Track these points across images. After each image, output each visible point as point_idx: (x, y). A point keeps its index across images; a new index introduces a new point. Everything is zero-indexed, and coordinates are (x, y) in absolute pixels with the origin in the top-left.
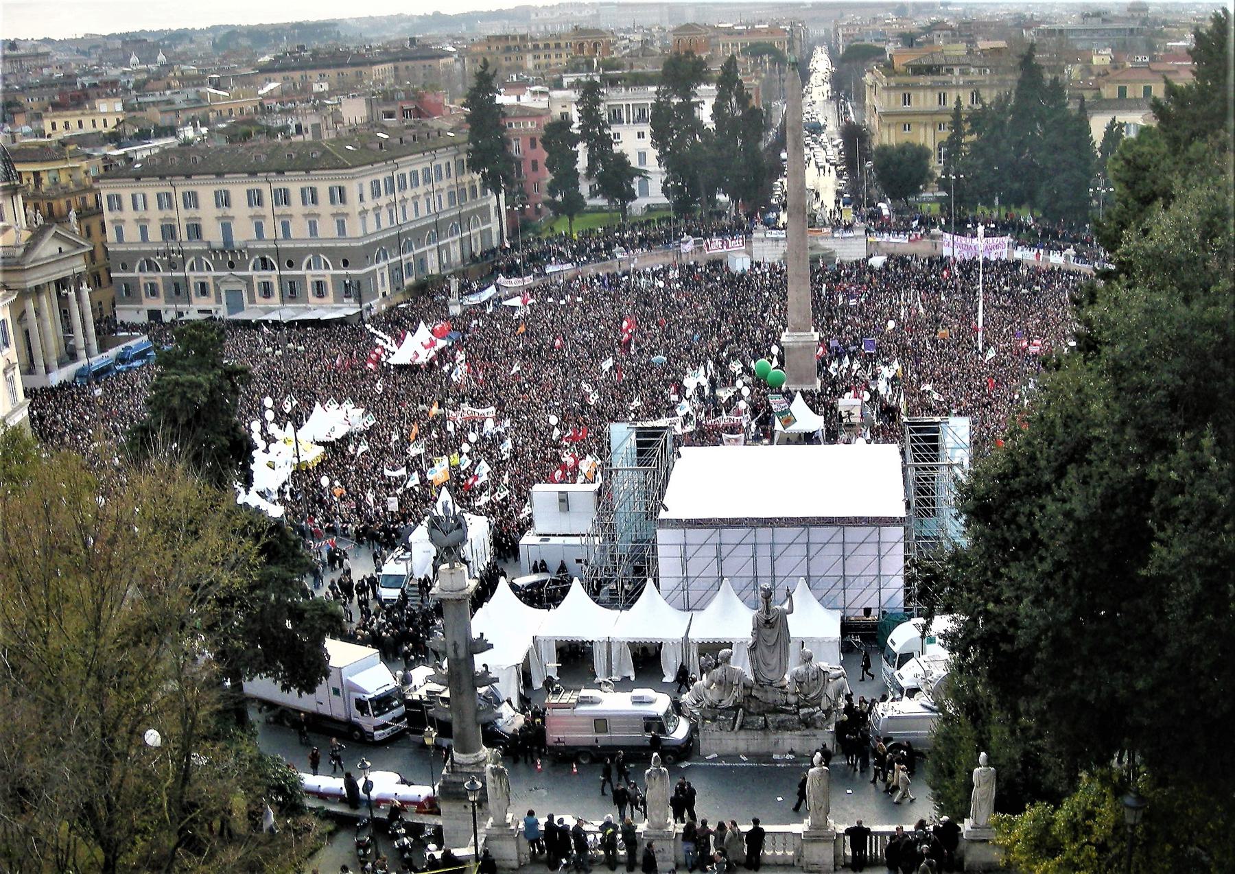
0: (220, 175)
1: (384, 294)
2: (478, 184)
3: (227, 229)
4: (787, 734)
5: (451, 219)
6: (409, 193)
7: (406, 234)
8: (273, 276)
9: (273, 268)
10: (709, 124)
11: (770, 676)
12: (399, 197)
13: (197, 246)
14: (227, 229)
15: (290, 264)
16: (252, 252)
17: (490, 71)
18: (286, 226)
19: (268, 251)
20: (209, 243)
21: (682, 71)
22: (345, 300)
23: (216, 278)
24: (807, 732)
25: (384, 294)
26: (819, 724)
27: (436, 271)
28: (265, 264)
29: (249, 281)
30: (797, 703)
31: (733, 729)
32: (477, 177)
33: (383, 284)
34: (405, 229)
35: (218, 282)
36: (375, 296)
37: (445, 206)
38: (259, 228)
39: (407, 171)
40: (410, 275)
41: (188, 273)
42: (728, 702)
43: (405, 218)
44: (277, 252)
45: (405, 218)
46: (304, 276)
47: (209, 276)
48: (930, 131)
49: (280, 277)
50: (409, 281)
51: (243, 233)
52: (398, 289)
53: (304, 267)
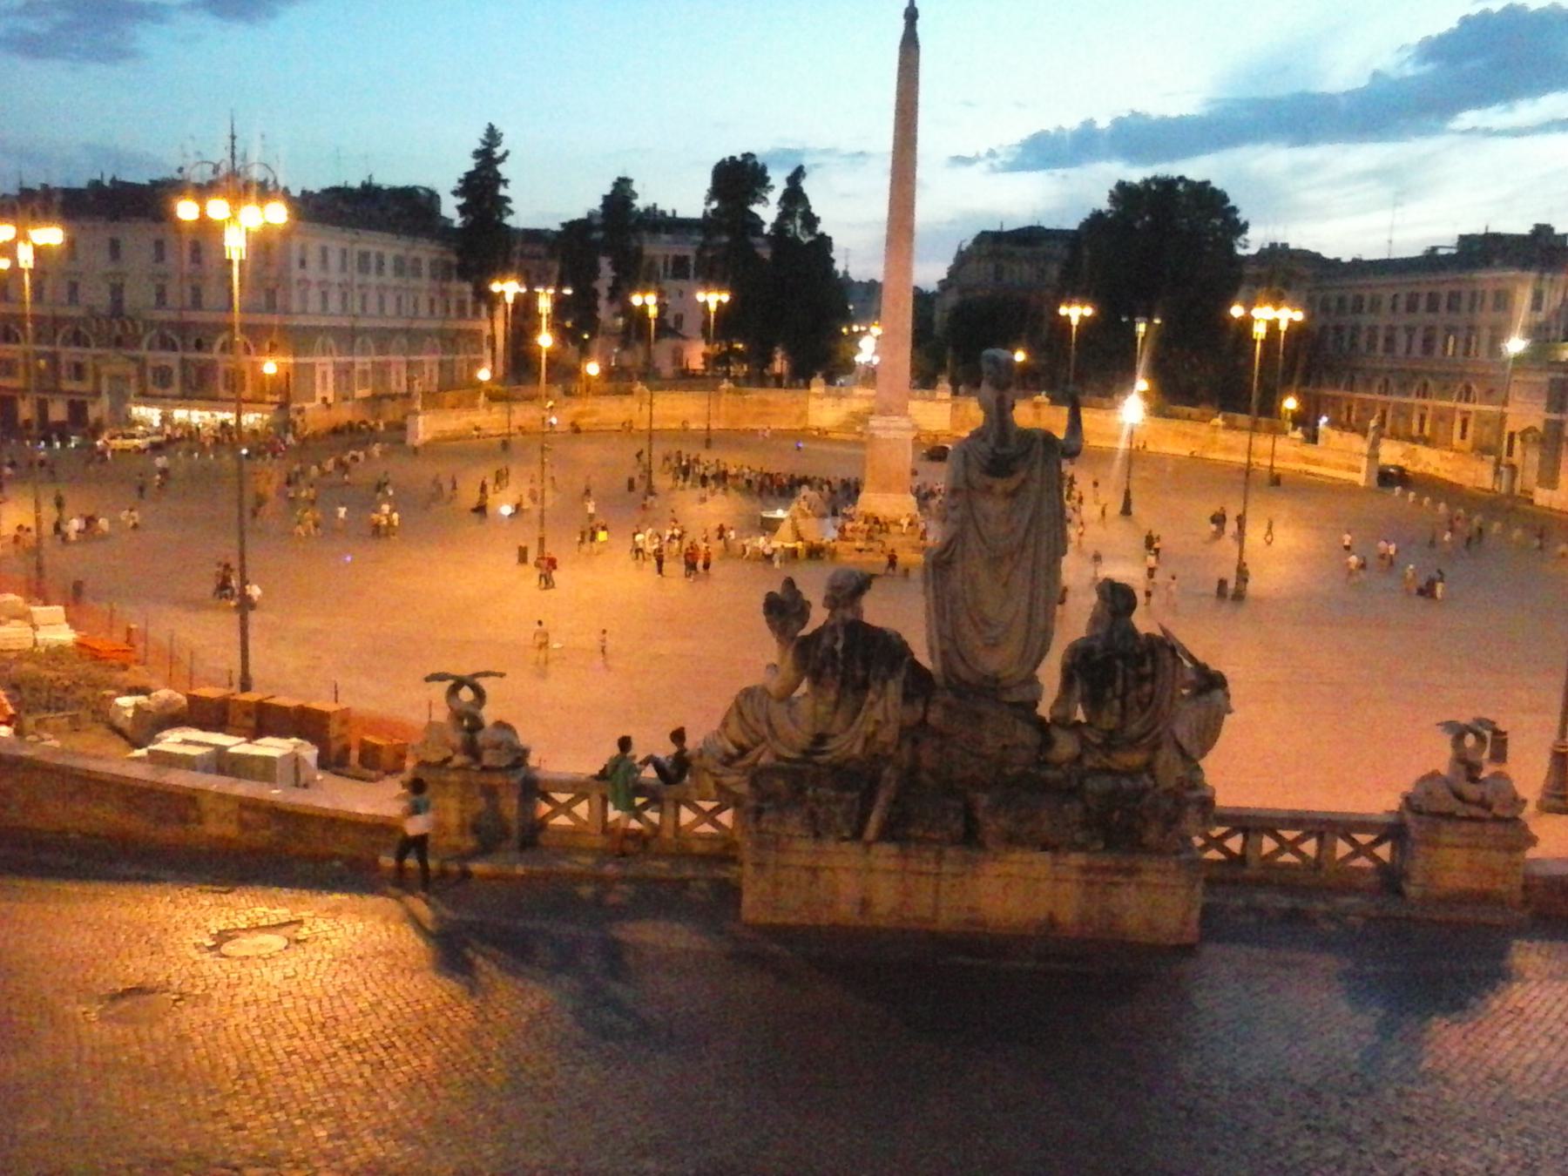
0: (115, 217)
1: (324, 400)
2: (470, 298)
3: (117, 291)
4: (1041, 862)
5: (428, 333)
6: (372, 279)
7: (365, 331)
8: (171, 359)
9: (174, 348)
10: (766, 253)
11: (994, 662)
13: (74, 312)
14: (117, 291)
15: (199, 346)
16: (149, 325)
17: (499, 151)
18: (197, 293)
19: (170, 324)
20: (91, 309)
21: (737, 179)
22: (269, 398)
23: (96, 357)
24: (1107, 861)
25: (324, 400)
26: (1152, 835)
27: (404, 389)
28: (166, 344)
29: (141, 363)
30: (1079, 759)
31: (858, 835)
33: (325, 388)
35: (98, 362)
36: (313, 399)
37: (424, 310)
38: (161, 295)
39: (373, 249)
40: (364, 385)
41: (59, 348)
42: (846, 745)
43: (364, 308)
44: (183, 328)
45: (364, 308)
46: (214, 362)
47: (86, 355)
49: (184, 363)
51: (138, 296)
52: (345, 399)
53: (217, 347)
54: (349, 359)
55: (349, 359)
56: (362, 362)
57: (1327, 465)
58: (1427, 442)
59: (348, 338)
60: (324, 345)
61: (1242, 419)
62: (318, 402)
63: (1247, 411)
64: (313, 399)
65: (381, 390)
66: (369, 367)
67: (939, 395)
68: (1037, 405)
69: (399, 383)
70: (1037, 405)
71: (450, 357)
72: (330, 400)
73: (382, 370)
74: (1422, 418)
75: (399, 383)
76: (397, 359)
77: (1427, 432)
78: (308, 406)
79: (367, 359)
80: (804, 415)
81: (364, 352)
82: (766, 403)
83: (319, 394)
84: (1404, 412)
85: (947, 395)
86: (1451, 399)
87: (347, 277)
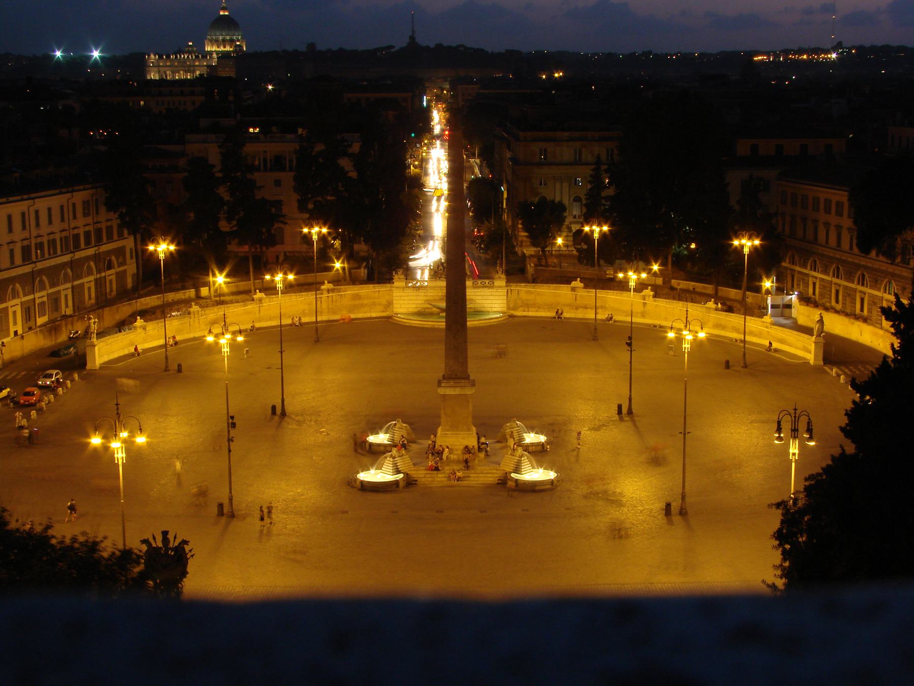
1: (16, 333)
5: (88, 258)
12: (34, 232)
25: (16, 333)
32: (113, 215)
33: (15, 323)
34: (40, 266)
40: (42, 314)
48: (565, 185)
50: (41, 321)
52: (30, 329)
54: (32, 297)
55: (32, 297)
56: (41, 296)
57: (790, 345)
58: (865, 320)
59: (30, 281)
60: (13, 290)
61: (733, 293)
62: (12, 334)
63: (739, 288)
64: (8, 335)
65: (56, 315)
66: (45, 299)
67: (497, 283)
68: (573, 289)
69: (67, 306)
70: (573, 289)
71: (103, 274)
72: (20, 332)
73: (55, 301)
74: (862, 300)
75: (67, 306)
76: (65, 289)
77: (865, 312)
78: (5, 340)
79: (44, 293)
80: (390, 304)
81: (42, 288)
82: (357, 297)
83: (12, 330)
84: (850, 294)
85: (503, 283)
86: (879, 290)
87: (26, 234)
